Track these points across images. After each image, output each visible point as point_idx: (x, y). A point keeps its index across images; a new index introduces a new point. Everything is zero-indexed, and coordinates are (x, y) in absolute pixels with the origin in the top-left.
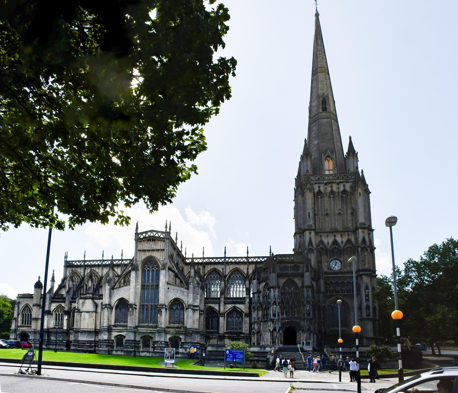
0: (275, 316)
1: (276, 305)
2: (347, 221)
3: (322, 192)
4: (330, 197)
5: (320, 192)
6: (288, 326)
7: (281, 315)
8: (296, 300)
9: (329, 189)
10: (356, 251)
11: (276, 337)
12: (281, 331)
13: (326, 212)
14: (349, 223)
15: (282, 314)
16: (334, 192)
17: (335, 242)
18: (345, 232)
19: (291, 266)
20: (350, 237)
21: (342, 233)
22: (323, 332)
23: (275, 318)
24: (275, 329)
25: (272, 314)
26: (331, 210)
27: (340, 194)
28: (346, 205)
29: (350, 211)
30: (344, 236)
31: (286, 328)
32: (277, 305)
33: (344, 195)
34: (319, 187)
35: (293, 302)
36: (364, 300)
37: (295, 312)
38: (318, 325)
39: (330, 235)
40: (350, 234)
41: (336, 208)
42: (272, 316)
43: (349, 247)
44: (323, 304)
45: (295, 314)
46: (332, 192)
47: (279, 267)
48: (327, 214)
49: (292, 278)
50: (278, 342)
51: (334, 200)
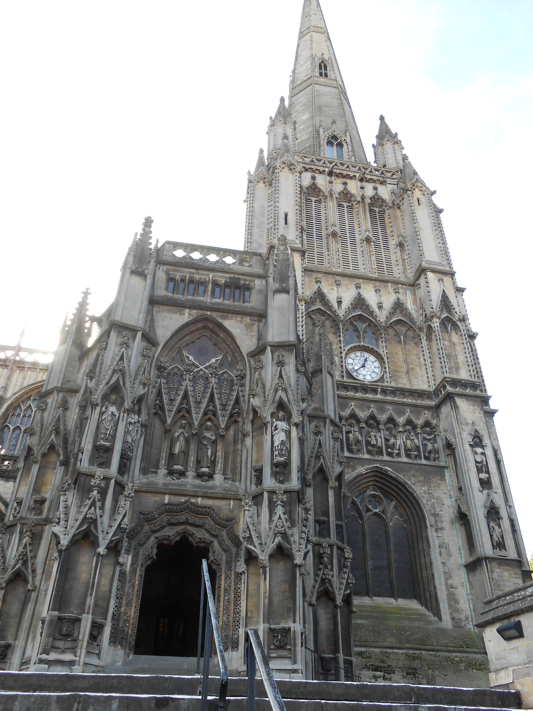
0: (106, 464)
1: (119, 404)
2: (389, 263)
3: (320, 190)
4: (340, 205)
5: (314, 189)
6: (171, 532)
7: (145, 471)
8: (224, 406)
9: (338, 186)
10: (423, 336)
11: (88, 587)
12: (127, 560)
13: (331, 229)
14: (395, 268)
15: (149, 467)
16: (352, 196)
17: (359, 302)
18: (387, 282)
19: (215, 284)
20: (401, 297)
21: (378, 284)
22: (339, 601)
23: (99, 472)
24: (86, 537)
25: (87, 445)
26: (343, 230)
27: (368, 201)
28: (384, 228)
29: (392, 243)
30: (383, 291)
31: (161, 547)
32: (127, 404)
33: (377, 210)
34: (313, 178)
35: (210, 414)
36: (476, 485)
37: (213, 463)
38: (319, 557)
39: (344, 281)
40: (401, 291)
41: (357, 230)
42: (85, 457)
43: (399, 321)
44: (338, 469)
45: (211, 476)
46: (346, 195)
47: (170, 279)
48: (334, 235)
49: (215, 315)
50: (97, 629)
51: (350, 212)
